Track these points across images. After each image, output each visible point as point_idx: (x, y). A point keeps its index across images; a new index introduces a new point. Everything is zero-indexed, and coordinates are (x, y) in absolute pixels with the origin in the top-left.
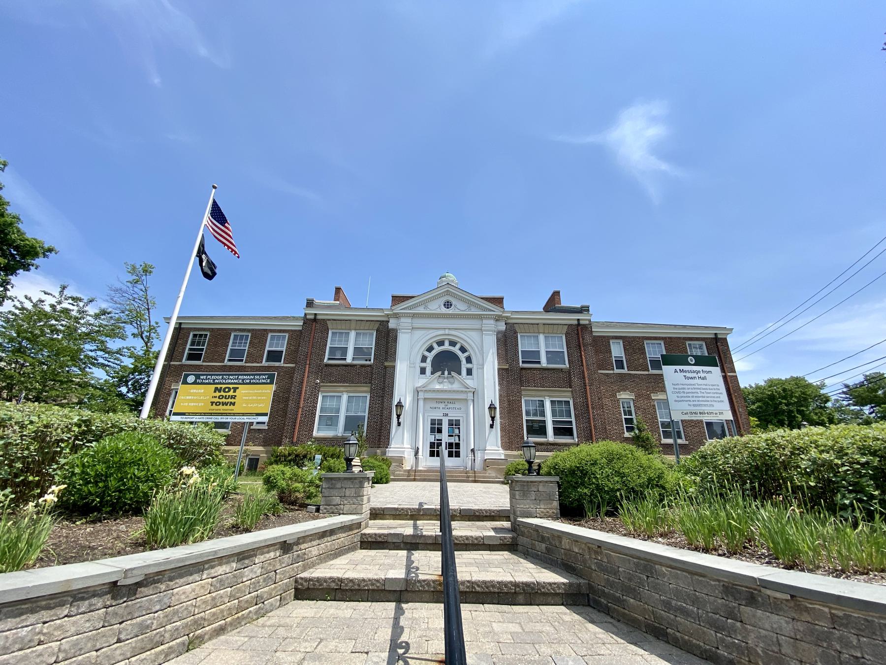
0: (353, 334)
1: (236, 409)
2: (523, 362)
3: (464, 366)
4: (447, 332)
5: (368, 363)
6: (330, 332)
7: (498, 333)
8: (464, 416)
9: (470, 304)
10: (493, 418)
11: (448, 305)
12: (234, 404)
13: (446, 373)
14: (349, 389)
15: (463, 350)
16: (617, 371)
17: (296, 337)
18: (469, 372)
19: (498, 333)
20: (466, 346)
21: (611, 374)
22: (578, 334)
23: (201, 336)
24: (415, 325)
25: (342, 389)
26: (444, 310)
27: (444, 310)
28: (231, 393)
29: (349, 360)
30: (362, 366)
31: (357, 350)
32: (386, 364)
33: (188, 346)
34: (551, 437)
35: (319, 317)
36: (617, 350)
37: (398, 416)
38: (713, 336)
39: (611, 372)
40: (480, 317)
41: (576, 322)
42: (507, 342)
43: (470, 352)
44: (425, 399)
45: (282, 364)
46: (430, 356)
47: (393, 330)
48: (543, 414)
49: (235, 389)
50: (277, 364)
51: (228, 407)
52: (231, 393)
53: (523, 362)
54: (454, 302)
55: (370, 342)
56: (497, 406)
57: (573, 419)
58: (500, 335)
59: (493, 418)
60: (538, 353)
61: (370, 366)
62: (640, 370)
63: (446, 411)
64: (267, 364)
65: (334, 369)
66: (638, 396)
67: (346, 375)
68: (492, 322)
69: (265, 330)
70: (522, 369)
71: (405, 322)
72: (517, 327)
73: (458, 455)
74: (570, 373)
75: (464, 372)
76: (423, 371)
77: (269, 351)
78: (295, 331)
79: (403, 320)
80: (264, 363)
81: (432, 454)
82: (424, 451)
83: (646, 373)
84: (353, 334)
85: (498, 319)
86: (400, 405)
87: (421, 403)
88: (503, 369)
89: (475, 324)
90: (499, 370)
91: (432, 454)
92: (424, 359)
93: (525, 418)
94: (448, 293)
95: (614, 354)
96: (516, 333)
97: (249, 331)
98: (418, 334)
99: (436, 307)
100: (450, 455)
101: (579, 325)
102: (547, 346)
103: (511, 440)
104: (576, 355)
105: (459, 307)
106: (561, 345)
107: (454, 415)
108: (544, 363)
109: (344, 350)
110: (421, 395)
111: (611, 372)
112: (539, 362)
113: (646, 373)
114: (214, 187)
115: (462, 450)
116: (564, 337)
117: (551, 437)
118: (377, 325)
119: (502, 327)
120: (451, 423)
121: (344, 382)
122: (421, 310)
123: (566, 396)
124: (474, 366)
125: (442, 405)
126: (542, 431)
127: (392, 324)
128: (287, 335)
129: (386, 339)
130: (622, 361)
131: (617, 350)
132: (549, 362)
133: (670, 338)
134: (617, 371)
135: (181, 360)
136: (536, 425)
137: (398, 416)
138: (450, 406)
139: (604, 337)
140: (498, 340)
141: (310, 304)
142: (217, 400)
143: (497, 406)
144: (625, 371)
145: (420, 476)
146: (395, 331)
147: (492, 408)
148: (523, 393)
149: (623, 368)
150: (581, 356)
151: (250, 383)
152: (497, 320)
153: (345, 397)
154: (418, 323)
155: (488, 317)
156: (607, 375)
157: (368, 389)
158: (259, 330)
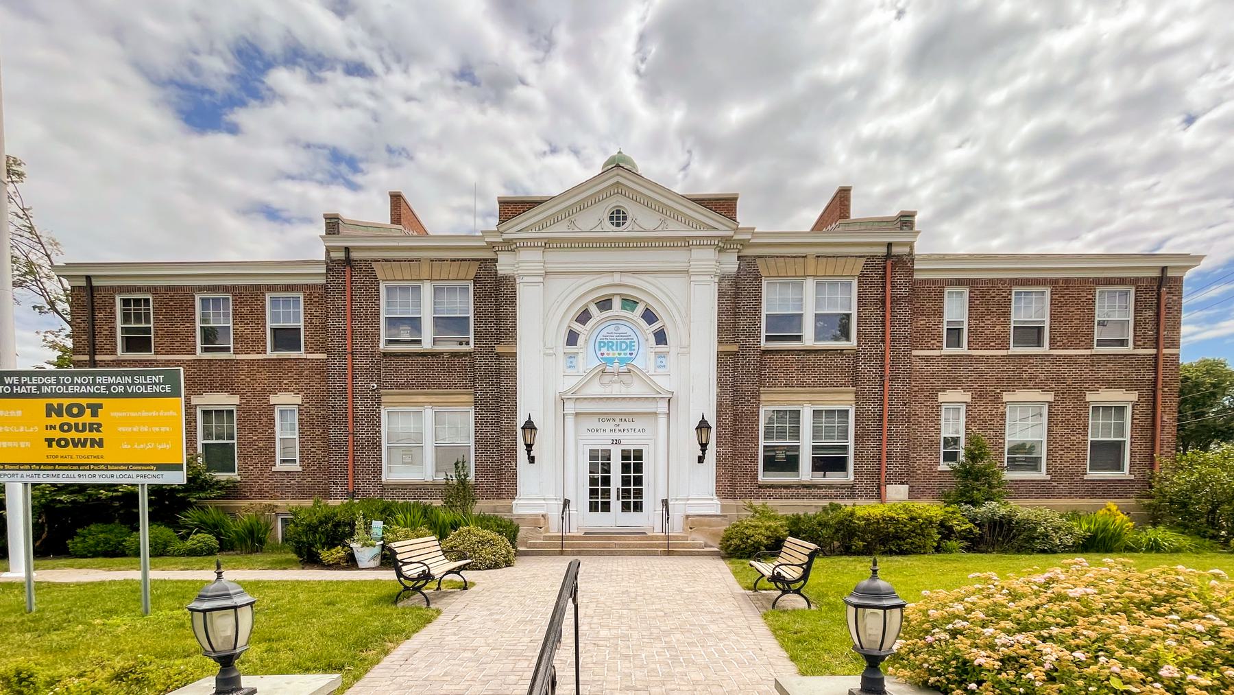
0: (427, 289)
2: (768, 338)
4: (617, 279)
5: (464, 348)
6: (382, 287)
7: (723, 278)
8: (652, 447)
9: (665, 211)
10: (704, 447)
11: (618, 218)
14: (433, 399)
17: (318, 297)
19: (723, 278)
20: (657, 309)
21: (932, 358)
22: (884, 276)
23: (137, 302)
24: (550, 267)
25: (421, 399)
26: (610, 231)
27: (610, 231)
29: (427, 344)
30: (454, 355)
31: (445, 324)
32: (499, 349)
33: (119, 324)
34: (806, 472)
35: (354, 255)
36: (956, 309)
37: (529, 447)
38: (1156, 274)
39: (936, 353)
40: (685, 243)
41: (883, 250)
42: (738, 299)
43: (664, 321)
45: (302, 354)
47: (506, 278)
48: (796, 433)
50: (293, 354)
54: (631, 209)
55: (464, 305)
56: (712, 422)
57: (851, 443)
58: (726, 284)
59: (704, 447)
61: (466, 354)
62: (993, 348)
63: (617, 436)
64: (275, 355)
65: (401, 362)
66: (979, 396)
67: (426, 374)
68: (710, 254)
72: (761, 266)
73: (638, 507)
74: (857, 357)
78: (315, 286)
80: (270, 354)
81: (593, 507)
82: (580, 498)
83: (1004, 352)
84: (427, 289)
85: (723, 245)
86: (529, 426)
87: (570, 421)
88: (727, 353)
89: (676, 258)
90: (720, 355)
91: (593, 507)
93: (762, 443)
94: (618, 188)
95: (946, 318)
96: (758, 277)
97: (225, 289)
98: (560, 285)
99: (594, 223)
100: (626, 507)
101: (889, 256)
103: (732, 481)
104: (875, 319)
105: (643, 222)
106: (846, 301)
107: (631, 442)
108: (809, 340)
109: (415, 323)
110: (570, 408)
111: (936, 353)
113: (1004, 352)
115: (646, 500)
116: (855, 283)
117: (806, 472)
118: (473, 270)
119: (730, 264)
120: (625, 456)
123: (845, 400)
125: (609, 425)
126: (791, 463)
127: (505, 264)
128: (301, 295)
129: (495, 298)
130: (959, 331)
131: (956, 309)
132: (818, 337)
133: (1066, 281)
134: (947, 351)
136: (781, 456)
137: (529, 447)
138: (623, 425)
139: (934, 281)
140: (721, 294)
141: (333, 224)
143: (712, 422)
144: (964, 350)
145: (571, 546)
146: (510, 281)
147: (703, 426)
148: (763, 397)
149: (959, 345)
150: (883, 323)
152: (721, 250)
153: (428, 413)
154: (558, 260)
155: (701, 242)
156: (927, 359)
157: (471, 398)
158: (246, 287)
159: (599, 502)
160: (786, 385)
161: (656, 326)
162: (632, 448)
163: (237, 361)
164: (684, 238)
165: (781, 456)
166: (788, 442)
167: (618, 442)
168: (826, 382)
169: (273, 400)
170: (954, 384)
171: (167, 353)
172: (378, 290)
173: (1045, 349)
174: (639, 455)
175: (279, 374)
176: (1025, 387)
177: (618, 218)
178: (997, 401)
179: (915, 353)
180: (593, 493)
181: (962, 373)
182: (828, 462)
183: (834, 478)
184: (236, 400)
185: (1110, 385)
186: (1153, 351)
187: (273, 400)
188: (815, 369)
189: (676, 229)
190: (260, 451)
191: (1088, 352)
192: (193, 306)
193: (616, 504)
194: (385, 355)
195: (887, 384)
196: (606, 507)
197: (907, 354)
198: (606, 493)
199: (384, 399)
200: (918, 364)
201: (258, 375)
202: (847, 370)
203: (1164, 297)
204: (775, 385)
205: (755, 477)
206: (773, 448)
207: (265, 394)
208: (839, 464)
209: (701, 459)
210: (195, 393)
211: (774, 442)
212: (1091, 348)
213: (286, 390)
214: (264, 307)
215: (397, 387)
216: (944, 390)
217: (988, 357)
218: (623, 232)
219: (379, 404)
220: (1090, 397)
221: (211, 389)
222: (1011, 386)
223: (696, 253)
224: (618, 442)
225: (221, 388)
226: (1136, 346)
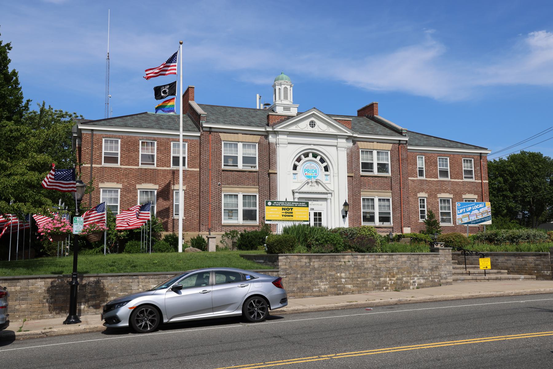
1: (294, 218)
4: (312, 147)
5: (253, 169)
6: (223, 143)
8: (325, 210)
11: (312, 124)
12: (292, 216)
14: (243, 189)
16: (420, 178)
19: (348, 149)
21: (415, 180)
26: (310, 130)
28: (290, 211)
31: (246, 160)
32: (270, 171)
39: (416, 179)
40: (335, 137)
41: (398, 142)
42: (352, 157)
48: (373, 206)
49: (292, 209)
51: (290, 217)
52: (290, 211)
55: (254, 152)
60: (372, 164)
66: (430, 195)
67: (241, 178)
69: (169, 139)
70: (362, 176)
71: (282, 138)
77: (173, 157)
79: (280, 137)
83: (436, 179)
93: (362, 211)
102: (378, 159)
104: (396, 166)
109: (235, 159)
111: (416, 179)
113: (436, 179)
114: (181, 43)
116: (389, 152)
117: (377, 222)
120: (315, 214)
121: (238, 184)
122: (293, 129)
123: (388, 195)
126: (372, 219)
127: (271, 139)
131: (421, 163)
132: (378, 171)
135: (101, 164)
136: (368, 215)
142: (284, 214)
144: (424, 178)
148: (362, 193)
151: (297, 206)
155: (341, 137)
156: (413, 181)
157: (257, 190)
161: (325, 164)
162: (318, 212)
164: (336, 135)
165: (368, 215)
166: (370, 211)
167: (313, 209)
168: (382, 188)
171: (126, 165)
173: (449, 179)
174: (320, 214)
176: (444, 192)
177: (312, 124)
178: (436, 197)
179: (409, 178)
181: (425, 187)
182: (384, 218)
183: (386, 224)
185: (470, 192)
186: (480, 181)
188: (379, 184)
189: (332, 131)
191: (461, 181)
192: (139, 145)
194: (223, 171)
195: (402, 190)
197: (407, 179)
199: (223, 189)
200: (410, 183)
202: (389, 185)
203: (482, 163)
205: (360, 224)
206: (366, 213)
208: (387, 219)
210: (138, 183)
212: (462, 179)
216: (419, 192)
218: (315, 130)
219: (221, 191)
221: (146, 182)
222: (440, 191)
223: (339, 140)
224: (313, 209)
225: (150, 182)
226: (475, 179)
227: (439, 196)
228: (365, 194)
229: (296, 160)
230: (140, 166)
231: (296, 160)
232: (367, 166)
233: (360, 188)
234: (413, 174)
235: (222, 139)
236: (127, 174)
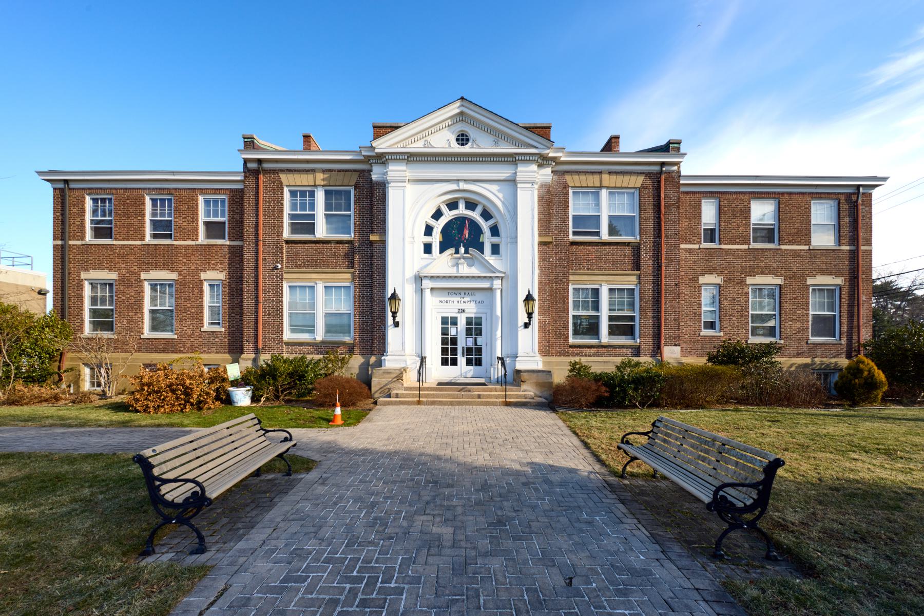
2: (575, 233)
3: (487, 240)
6: (286, 190)
8: (489, 315)
10: (530, 315)
13: (462, 250)
15: (486, 215)
16: (705, 245)
18: (496, 249)
34: (605, 336)
36: (709, 213)
44: (432, 289)
46: (439, 226)
48: (596, 306)
53: (575, 233)
56: (536, 295)
57: (636, 314)
60: (598, 218)
62: (738, 243)
65: (299, 247)
66: (729, 280)
75: (488, 248)
76: (428, 249)
80: (202, 239)
81: (444, 362)
87: (427, 293)
91: (444, 362)
92: (429, 231)
93: (572, 313)
110: (427, 284)
111: (697, 246)
112: (597, 234)
117: (605, 336)
118: (354, 178)
121: (316, 266)
123: (629, 281)
124: (502, 241)
125: (456, 299)
148: (571, 278)
153: (320, 288)
156: (690, 251)
159: (449, 359)
160: (588, 269)
163: (177, 247)
167: (463, 311)
168: (615, 268)
169: (203, 276)
170: (711, 271)
171: (123, 239)
172: (282, 193)
175: (206, 255)
176: (762, 273)
178: (742, 283)
179: (682, 246)
180: (444, 351)
181: (715, 263)
182: (621, 327)
184: (174, 276)
185: (824, 272)
187: (203, 276)
190: (192, 316)
192: (143, 204)
193: (462, 360)
196: (454, 362)
197: (677, 247)
198: (454, 351)
200: (683, 255)
201: (193, 257)
204: (580, 269)
207: (197, 272)
209: (526, 325)
210: (144, 270)
211: (582, 313)
213: (213, 269)
214: (197, 205)
215: (296, 267)
216: (703, 274)
217: (735, 250)
219: (282, 279)
220: (810, 281)
221: (157, 267)
222: (753, 272)
224: (463, 311)
227: (749, 280)
228: (577, 284)
229: (433, 217)
230: (148, 239)
231: (433, 217)
232: (588, 223)
233: (568, 267)
234: (692, 236)
235: (284, 183)
236: (125, 254)
